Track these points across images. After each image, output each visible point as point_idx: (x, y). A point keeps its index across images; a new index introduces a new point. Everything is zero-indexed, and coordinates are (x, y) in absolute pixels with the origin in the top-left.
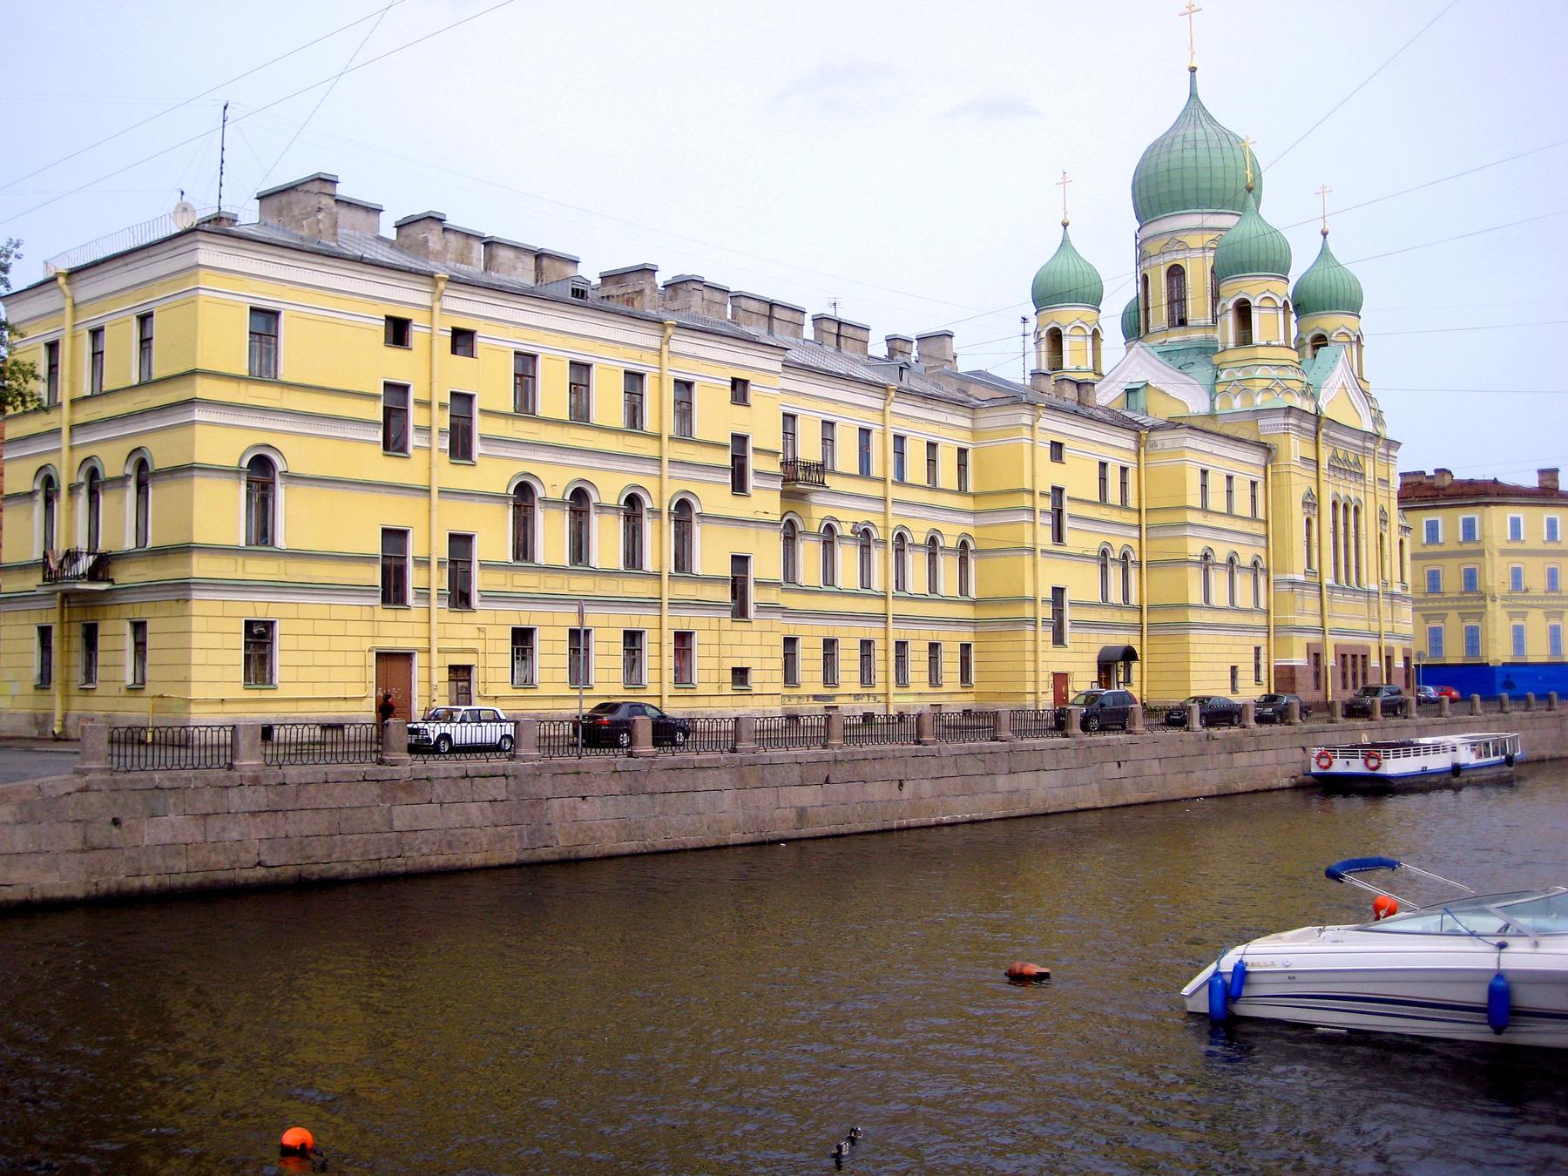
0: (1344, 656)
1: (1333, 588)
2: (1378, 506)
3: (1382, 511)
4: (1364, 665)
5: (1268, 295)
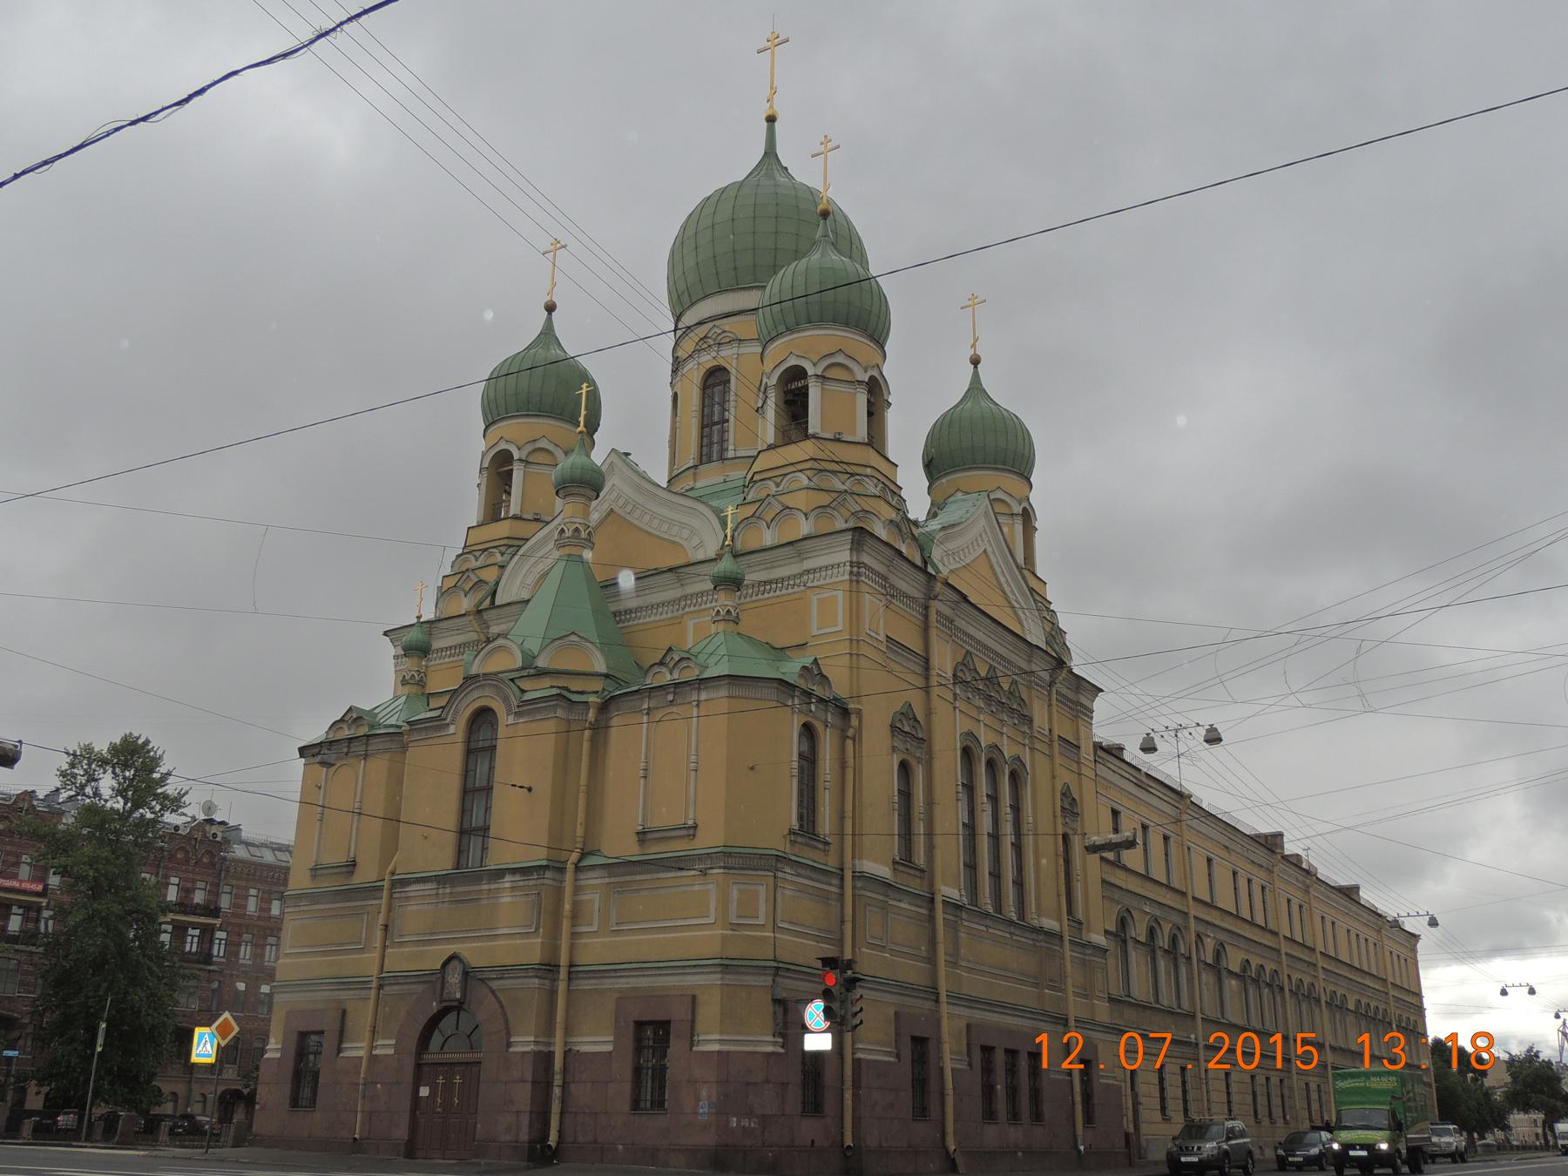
0: (987, 1050)
1: (958, 907)
2: (1059, 787)
3: (1066, 793)
4: (1035, 1070)
5: (840, 359)
